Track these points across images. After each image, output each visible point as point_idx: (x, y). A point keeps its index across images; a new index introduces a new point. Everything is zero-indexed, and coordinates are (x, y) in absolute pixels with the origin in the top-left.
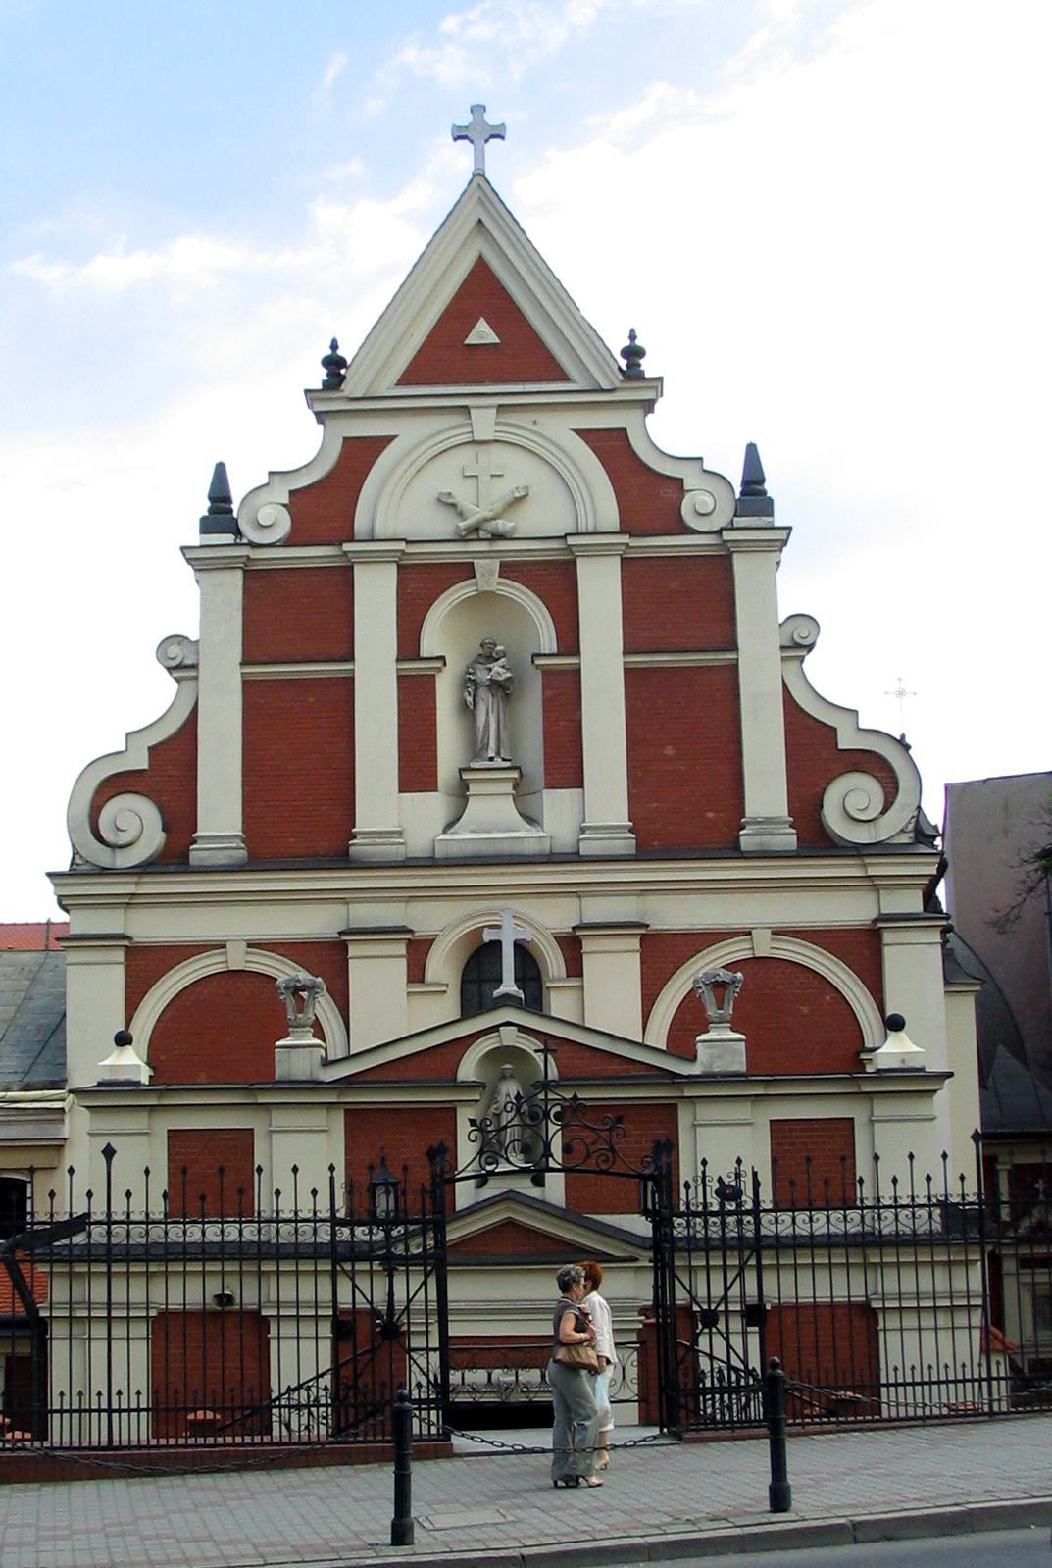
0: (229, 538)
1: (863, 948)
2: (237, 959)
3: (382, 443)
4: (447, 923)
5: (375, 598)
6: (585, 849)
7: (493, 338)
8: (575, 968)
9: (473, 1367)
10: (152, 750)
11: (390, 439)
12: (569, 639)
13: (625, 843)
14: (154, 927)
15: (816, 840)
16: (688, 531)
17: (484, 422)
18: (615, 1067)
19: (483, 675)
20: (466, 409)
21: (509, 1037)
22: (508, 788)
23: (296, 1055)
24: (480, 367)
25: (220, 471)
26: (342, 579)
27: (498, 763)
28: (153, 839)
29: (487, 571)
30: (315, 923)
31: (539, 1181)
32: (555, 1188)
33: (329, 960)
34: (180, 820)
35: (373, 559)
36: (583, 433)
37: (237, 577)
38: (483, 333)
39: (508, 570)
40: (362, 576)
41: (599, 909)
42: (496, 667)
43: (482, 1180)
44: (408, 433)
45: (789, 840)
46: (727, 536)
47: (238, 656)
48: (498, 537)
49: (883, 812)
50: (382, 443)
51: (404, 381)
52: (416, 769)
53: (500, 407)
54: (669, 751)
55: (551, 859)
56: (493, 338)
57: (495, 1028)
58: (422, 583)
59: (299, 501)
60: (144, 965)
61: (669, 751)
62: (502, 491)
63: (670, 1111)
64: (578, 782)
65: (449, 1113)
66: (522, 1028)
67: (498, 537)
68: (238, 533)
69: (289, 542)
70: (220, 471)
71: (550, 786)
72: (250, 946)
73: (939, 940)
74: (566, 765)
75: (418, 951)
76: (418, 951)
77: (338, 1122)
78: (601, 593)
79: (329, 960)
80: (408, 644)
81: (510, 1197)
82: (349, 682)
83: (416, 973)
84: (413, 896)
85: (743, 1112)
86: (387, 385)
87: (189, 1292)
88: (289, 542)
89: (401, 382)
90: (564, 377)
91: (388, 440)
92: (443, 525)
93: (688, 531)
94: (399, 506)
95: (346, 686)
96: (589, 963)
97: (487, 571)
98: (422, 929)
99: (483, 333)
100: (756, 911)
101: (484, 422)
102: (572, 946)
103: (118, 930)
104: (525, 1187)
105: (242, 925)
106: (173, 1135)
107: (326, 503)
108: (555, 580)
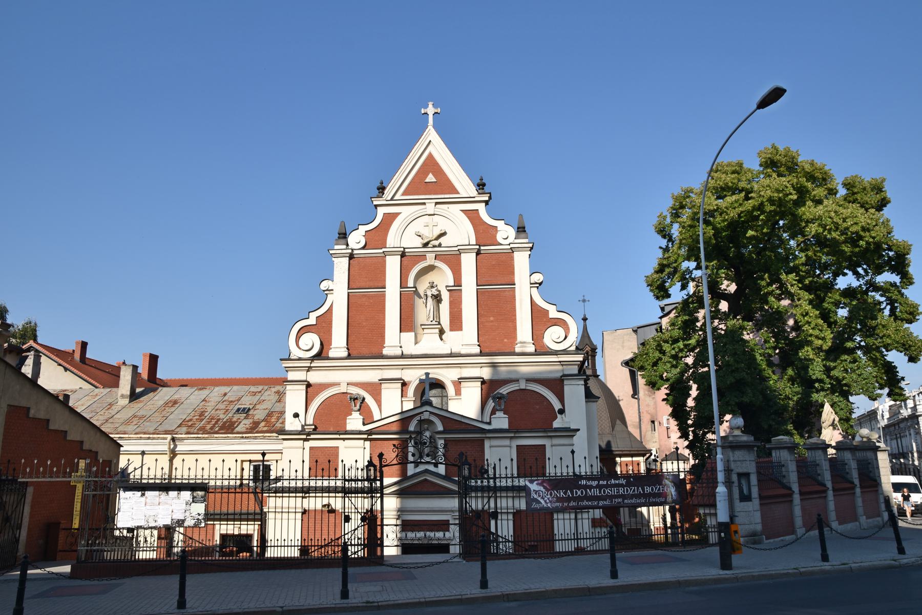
0: (344, 247)
2: (343, 389)
3: (397, 215)
4: (413, 376)
5: (393, 265)
6: (463, 352)
8: (458, 392)
9: (438, 531)
11: (399, 214)
12: (458, 282)
13: (477, 350)
14: (315, 377)
15: (542, 350)
17: (430, 207)
18: (463, 426)
19: (429, 293)
20: (424, 204)
21: (426, 416)
22: (437, 331)
23: (354, 422)
24: (429, 189)
27: (434, 323)
29: (430, 260)
30: (372, 376)
31: (436, 465)
32: (441, 469)
33: (375, 389)
35: (392, 253)
38: (431, 178)
40: (389, 259)
42: (434, 290)
43: (417, 464)
44: (406, 212)
46: (512, 246)
48: (434, 246)
50: (397, 215)
51: (403, 195)
53: (437, 203)
54: (492, 319)
55: (451, 355)
56: (434, 180)
57: (422, 413)
61: (492, 319)
62: (437, 232)
63: (481, 442)
66: (431, 413)
67: (434, 246)
68: (347, 245)
69: (363, 248)
71: (451, 330)
73: (583, 382)
74: (456, 323)
75: (404, 384)
79: (375, 389)
80: (403, 284)
81: (427, 471)
83: (403, 395)
84: (403, 367)
85: (507, 442)
87: (315, 503)
88: (363, 248)
89: (403, 195)
90: (458, 193)
91: (398, 214)
92: (418, 242)
95: (383, 296)
96: (463, 390)
101: (430, 207)
102: (458, 383)
104: (431, 468)
105: (343, 378)
106: (311, 448)
108: (453, 260)
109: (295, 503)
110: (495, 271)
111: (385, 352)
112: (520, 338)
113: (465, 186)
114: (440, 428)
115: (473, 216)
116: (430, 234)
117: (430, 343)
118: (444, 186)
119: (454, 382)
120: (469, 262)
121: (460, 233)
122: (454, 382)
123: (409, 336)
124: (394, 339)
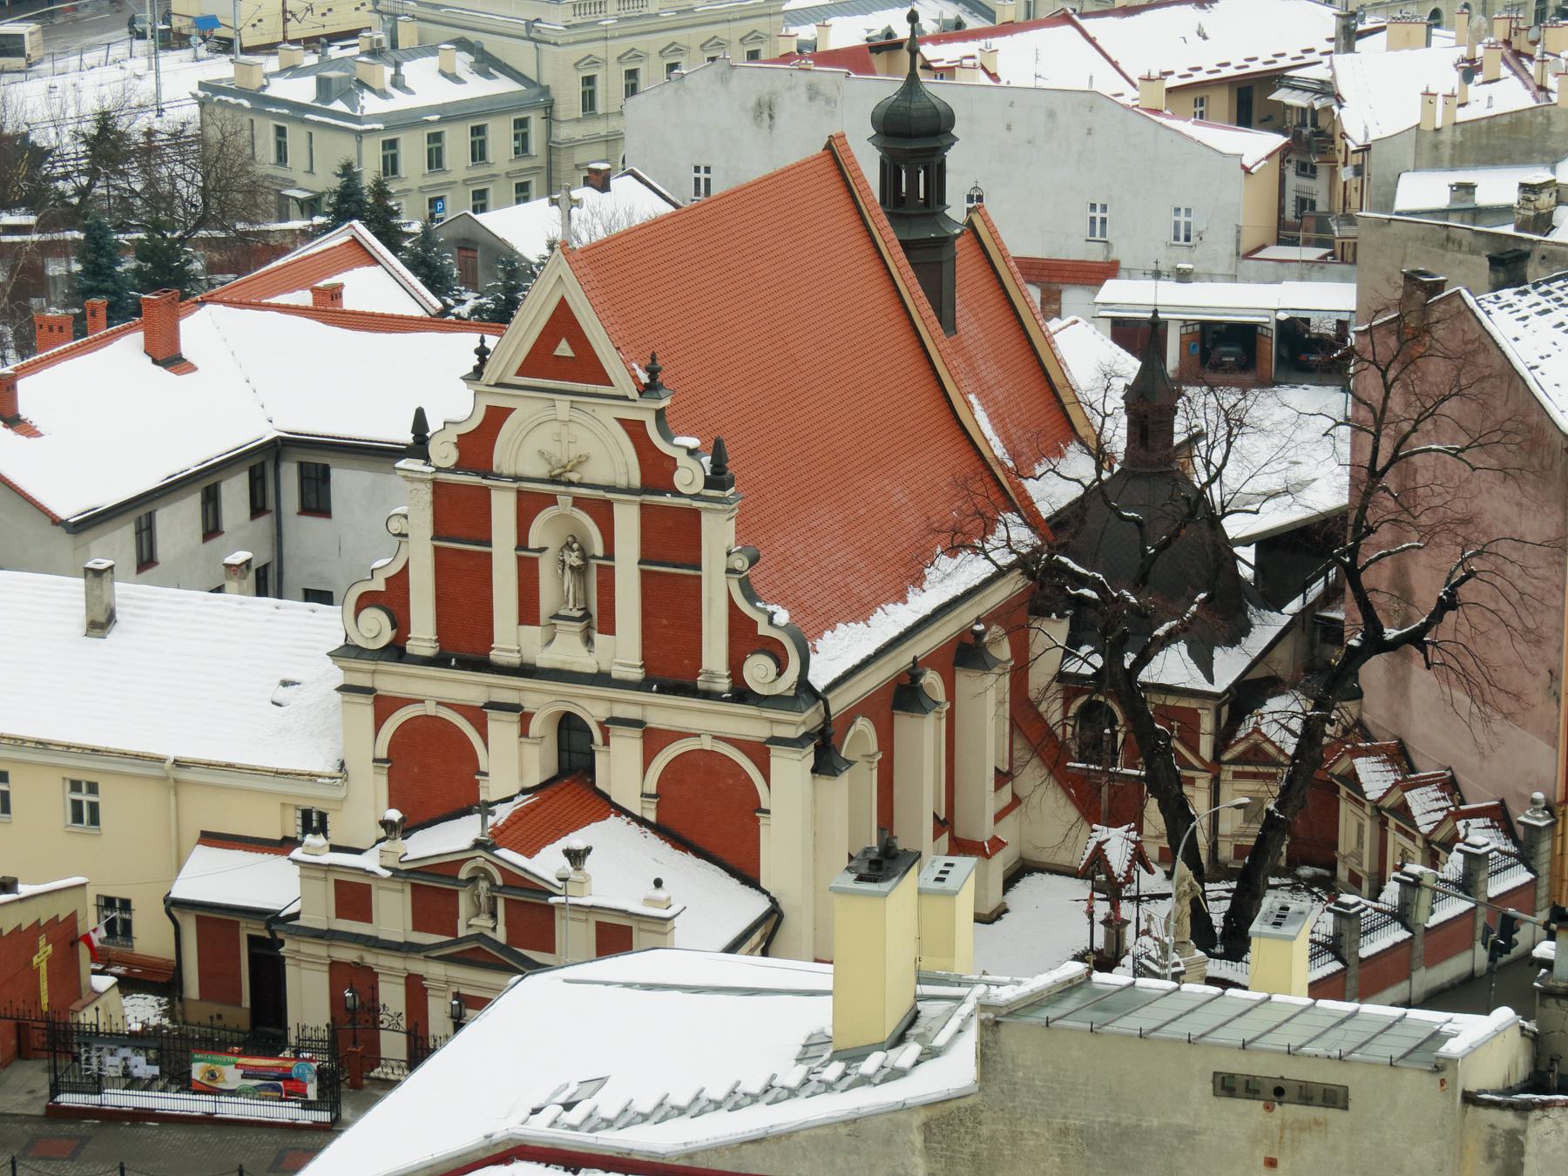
1: (760, 752)
2: (430, 709)
3: (507, 412)
7: (569, 353)
8: (606, 742)
10: (387, 580)
12: (609, 554)
13: (637, 674)
16: (677, 494)
21: (480, 862)
24: (562, 369)
25: (420, 417)
26: (484, 495)
28: (387, 635)
29: (565, 502)
34: (400, 623)
36: (622, 422)
37: (430, 485)
38: (564, 349)
39: (578, 502)
41: (621, 711)
45: (723, 685)
47: (429, 532)
49: (779, 674)
50: (507, 412)
52: (528, 613)
54: (665, 622)
56: (569, 353)
58: (529, 506)
59: (463, 442)
60: (384, 706)
61: (665, 622)
64: (612, 632)
65: (456, 893)
67: (570, 483)
70: (420, 417)
72: (439, 703)
76: (526, 719)
77: (408, 889)
78: (627, 520)
80: (522, 544)
82: (490, 555)
83: (524, 733)
85: (583, 917)
86: (511, 378)
87: (348, 954)
89: (519, 373)
90: (611, 384)
93: (677, 494)
94: (518, 452)
96: (612, 740)
97: (565, 502)
98: (528, 708)
99: (564, 349)
100: (705, 725)
103: (368, 684)
107: (477, 446)
108: (603, 514)
109: (320, 950)
110: (673, 538)
111: (496, 656)
112: (705, 665)
113: (621, 373)
114: (499, 882)
115: (635, 430)
116: (563, 453)
117: (567, 651)
118: (587, 368)
119: (601, 725)
120: (627, 520)
121: (615, 462)
122: (601, 725)
123: (534, 633)
124: (510, 638)
